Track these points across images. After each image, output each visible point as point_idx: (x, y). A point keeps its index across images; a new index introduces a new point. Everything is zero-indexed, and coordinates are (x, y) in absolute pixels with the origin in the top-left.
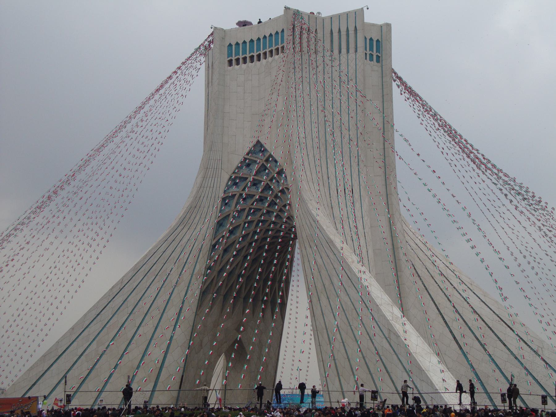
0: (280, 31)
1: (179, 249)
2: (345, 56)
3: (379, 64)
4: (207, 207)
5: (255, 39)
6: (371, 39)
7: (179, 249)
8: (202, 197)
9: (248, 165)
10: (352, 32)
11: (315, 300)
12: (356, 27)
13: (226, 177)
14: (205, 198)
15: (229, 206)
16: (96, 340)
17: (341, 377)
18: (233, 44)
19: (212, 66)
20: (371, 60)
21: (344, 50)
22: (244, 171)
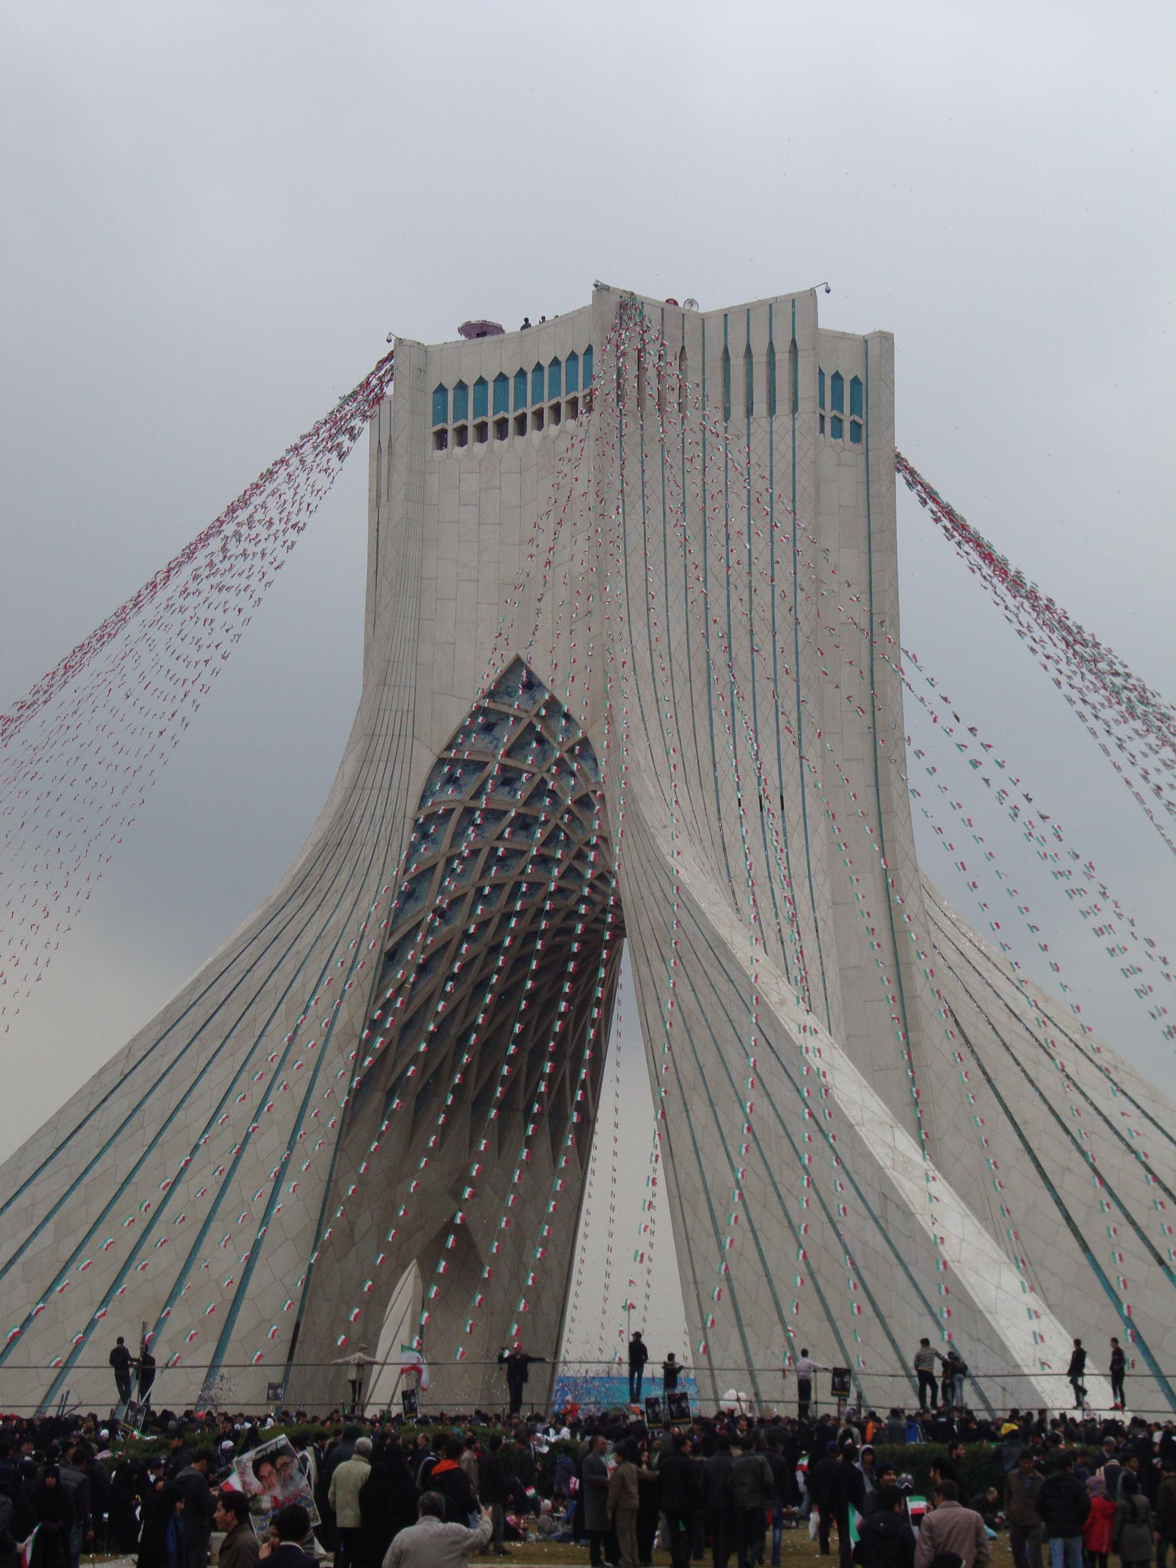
0: (580, 352)
1: (290, 965)
2: (764, 423)
3: (859, 447)
5: (511, 373)
6: (837, 377)
7: (290, 965)
8: (357, 819)
9: (489, 728)
10: (782, 357)
11: (674, 1109)
12: (794, 342)
13: (426, 761)
14: (366, 819)
15: (434, 842)
17: (747, 1330)
18: (450, 385)
19: (390, 446)
20: (837, 433)
21: (760, 407)
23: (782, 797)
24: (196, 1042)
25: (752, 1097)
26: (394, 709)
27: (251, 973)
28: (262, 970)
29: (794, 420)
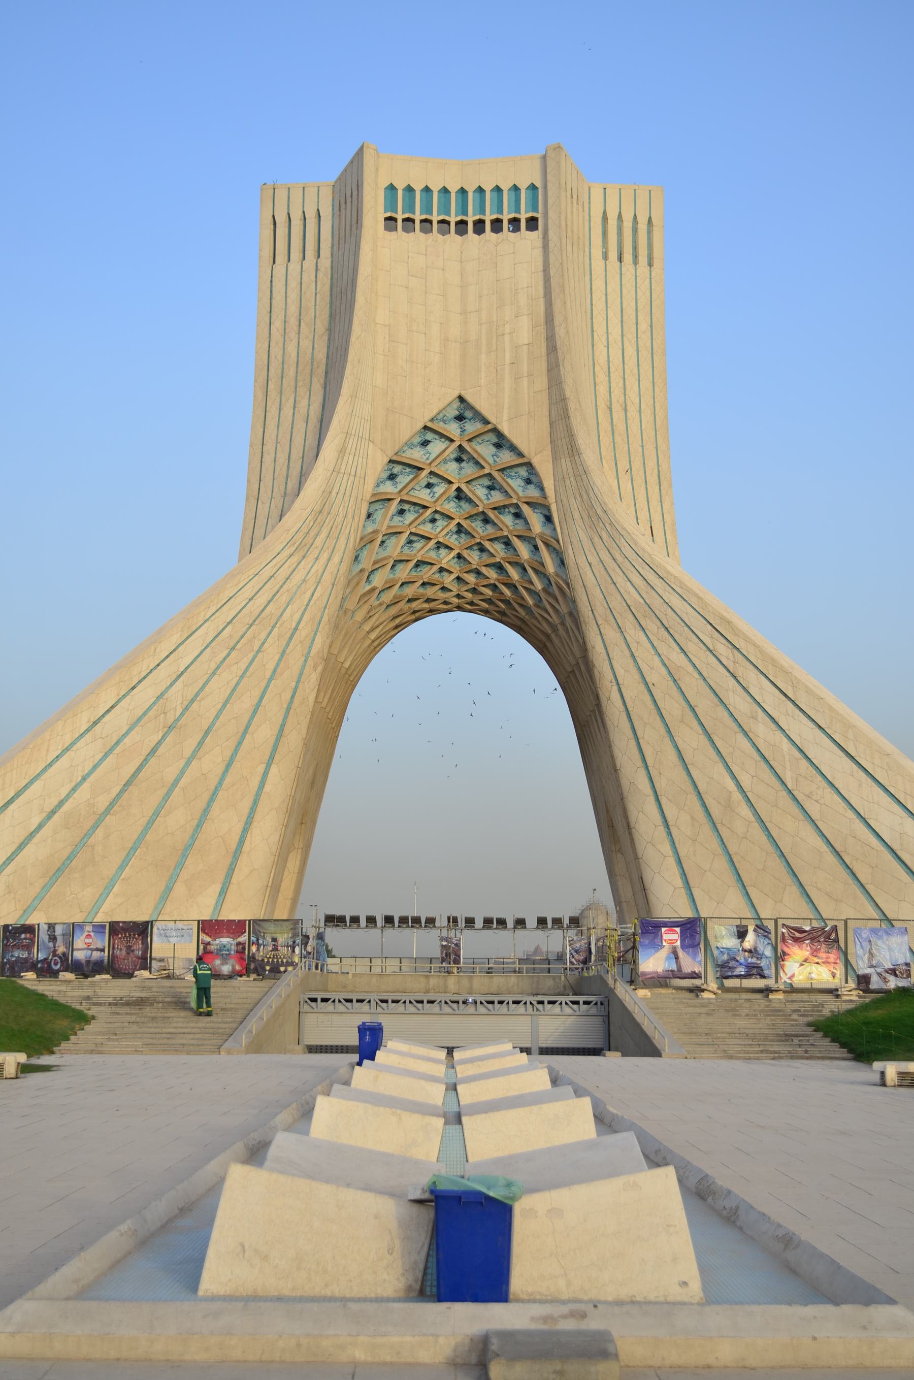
1: (283, 598)
2: (631, 268)
4: (342, 514)
5: (453, 188)
7: (283, 598)
9: (425, 443)
12: (650, 218)
14: (340, 496)
15: (374, 521)
16: (92, 778)
18: (400, 186)
21: (628, 256)
22: (416, 455)
25: (763, 731)
27: (252, 601)
28: (261, 600)
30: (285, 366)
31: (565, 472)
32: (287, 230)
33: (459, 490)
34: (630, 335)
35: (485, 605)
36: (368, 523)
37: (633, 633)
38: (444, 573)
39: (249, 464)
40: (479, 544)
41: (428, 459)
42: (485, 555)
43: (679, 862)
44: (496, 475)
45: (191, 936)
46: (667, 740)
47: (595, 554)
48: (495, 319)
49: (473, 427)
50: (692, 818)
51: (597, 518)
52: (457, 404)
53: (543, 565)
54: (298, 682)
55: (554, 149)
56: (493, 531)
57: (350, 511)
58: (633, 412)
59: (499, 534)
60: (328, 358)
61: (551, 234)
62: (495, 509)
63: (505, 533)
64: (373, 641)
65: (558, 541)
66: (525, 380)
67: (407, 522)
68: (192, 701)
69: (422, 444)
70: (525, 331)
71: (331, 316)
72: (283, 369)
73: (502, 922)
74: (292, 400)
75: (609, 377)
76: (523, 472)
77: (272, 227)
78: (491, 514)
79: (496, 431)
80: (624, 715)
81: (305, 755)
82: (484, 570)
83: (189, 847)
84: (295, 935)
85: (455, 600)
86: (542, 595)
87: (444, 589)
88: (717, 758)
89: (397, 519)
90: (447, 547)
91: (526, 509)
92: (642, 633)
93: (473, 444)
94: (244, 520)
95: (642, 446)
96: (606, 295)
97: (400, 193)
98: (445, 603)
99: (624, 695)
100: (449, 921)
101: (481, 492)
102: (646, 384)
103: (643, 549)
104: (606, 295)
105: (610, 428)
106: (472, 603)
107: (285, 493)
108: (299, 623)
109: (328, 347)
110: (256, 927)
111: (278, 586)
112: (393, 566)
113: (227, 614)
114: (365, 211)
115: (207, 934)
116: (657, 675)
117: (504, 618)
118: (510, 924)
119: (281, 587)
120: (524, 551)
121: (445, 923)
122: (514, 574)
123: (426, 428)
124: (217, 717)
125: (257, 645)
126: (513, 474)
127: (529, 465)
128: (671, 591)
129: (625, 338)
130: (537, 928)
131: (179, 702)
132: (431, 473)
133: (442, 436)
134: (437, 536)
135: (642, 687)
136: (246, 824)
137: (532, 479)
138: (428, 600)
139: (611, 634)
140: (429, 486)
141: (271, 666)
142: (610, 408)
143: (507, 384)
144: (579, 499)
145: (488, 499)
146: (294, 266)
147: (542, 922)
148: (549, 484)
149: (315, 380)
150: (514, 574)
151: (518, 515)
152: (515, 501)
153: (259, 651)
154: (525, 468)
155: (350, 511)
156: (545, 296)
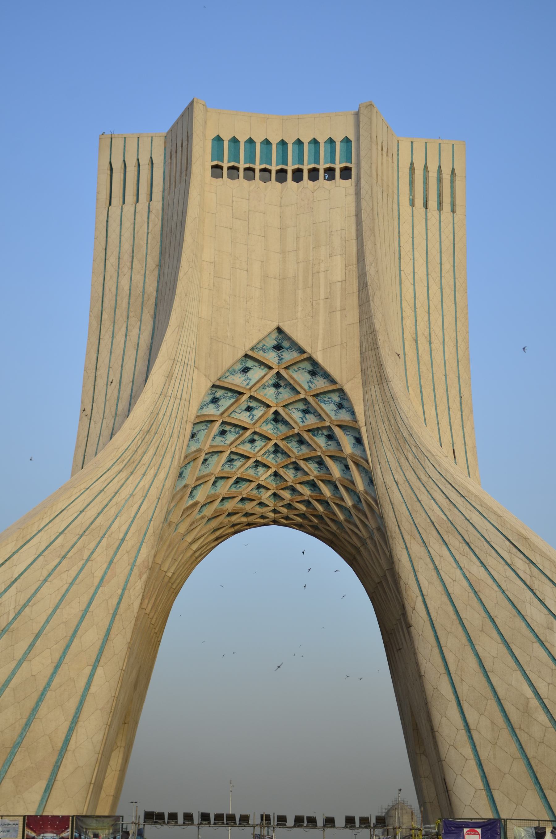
1: (112, 511)
2: (436, 214)
4: (168, 434)
5: (275, 140)
7: (112, 511)
8: (161, 415)
9: (246, 370)
10: (446, 177)
12: (453, 169)
14: (167, 417)
15: (197, 441)
18: (226, 138)
21: (433, 204)
22: (238, 381)
23: (454, 450)
24: (41, 557)
26: (186, 345)
27: (83, 514)
28: (91, 512)
29: (453, 217)
30: (119, 298)
31: (374, 398)
32: (122, 175)
33: (276, 413)
34: (434, 274)
35: (299, 520)
36: (192, 442)
37: (436, 548)
38: (262, 490)
39: (83, 387)
40: (295, 463)
41: (248, 384)
42: (299, 474)
43: (480, 765)
44: (310, 399)
45: (16, 831)
46: (468, 648)
47: (402, 474)
48: (311, 258)
49: (289, 356)
50: (492, 722)
51: (403, 440)
52: (275, 335)
53: (353, 483)
54: (124, 589)
55: (367, 107)
56: (307, 451)
57: (176, 431)
58: (437, 344)
59: (313, 454)
60: (157, 291)
61: (363, 182)
62: (309, 431)
63: (319, 454)
64: (195, 552)
65: (367, 461)
66: (338, 314)
67: (228, 442)
68: (25, 606)
69: (243, 371)
70: (338, 269)
71: (162, 254)
72: (116, 301)
73: (312, 821)
74: (124, 329)
75: (415, 312)
76: (336, 398)
77: (109, 172)
78: (306, 436)
79: (310, 359)
80: (428, 624)
81: (129, 658)
82: (299, 487)
83: (17, 745)
84: (115, 831)
85: (272, 515)
86: (353, 511)
87: (261, 504)
88: (516, 667)
89: (219, 439)
90: (265, 466)
91: (338, 432)
92: (444, 548)
93: (290, 371)
94: (78, 438)
95: (446, 375)
96: (413, 238)
97: (226, 144)
98: (262, 517)
99: (429, 605)
100: (262, 819)
101: (297, 415)
102: (449, 318)
103: (446, 470)
104: (413, 238)
105: (415, 359)
106: (287, 518)
107: (116, 414)
108: (126, 534)
109: (158, 282)
110: (79, 823)
111: (108, 500)
112: (215, 482)
113: (60, 524)
114: (194, 159)
115: (32, 829)
116: (459, 588)
117: (316, 532)
118: (320, 823)
119: (111, 500)
120: (336, 471)
121: (258, 821)
122: (326, 491)
123: (246, 356)
124: (47, 621)
125: (86, 554)
126: (326, 399)
127: (341, 391)
128: (472, 509)
129: (430, 277)
130: (346, 827)
131: (12, 607)
132: (251, 397)
133: (261, 363)
134: (255, 455)
135: (445, 598)
136: (72, 723)
137: (344, 404)
138: (247, 515)
139: (416, 548)
140: (249, 409)
141: (99, 574)
142: (416, 340)
143: (322, 317)
144: (387, 423)
145: (303, 422)
146: (129, 208)
147: (350, 821)
148: (359, 409)
149: (145, 311)
150: (326, 491)
151: (331, 437)
152: (328, 424)
153: (88, 560)
154: (337, 394)
155: (176, 431)
156: (357, 238)
